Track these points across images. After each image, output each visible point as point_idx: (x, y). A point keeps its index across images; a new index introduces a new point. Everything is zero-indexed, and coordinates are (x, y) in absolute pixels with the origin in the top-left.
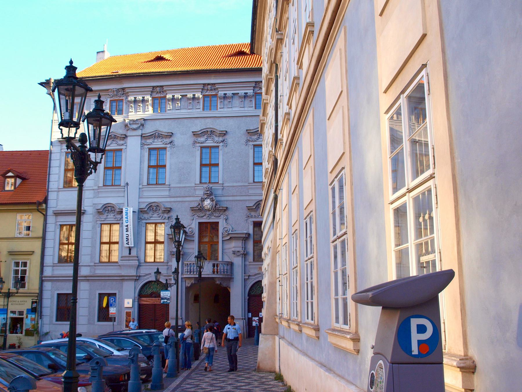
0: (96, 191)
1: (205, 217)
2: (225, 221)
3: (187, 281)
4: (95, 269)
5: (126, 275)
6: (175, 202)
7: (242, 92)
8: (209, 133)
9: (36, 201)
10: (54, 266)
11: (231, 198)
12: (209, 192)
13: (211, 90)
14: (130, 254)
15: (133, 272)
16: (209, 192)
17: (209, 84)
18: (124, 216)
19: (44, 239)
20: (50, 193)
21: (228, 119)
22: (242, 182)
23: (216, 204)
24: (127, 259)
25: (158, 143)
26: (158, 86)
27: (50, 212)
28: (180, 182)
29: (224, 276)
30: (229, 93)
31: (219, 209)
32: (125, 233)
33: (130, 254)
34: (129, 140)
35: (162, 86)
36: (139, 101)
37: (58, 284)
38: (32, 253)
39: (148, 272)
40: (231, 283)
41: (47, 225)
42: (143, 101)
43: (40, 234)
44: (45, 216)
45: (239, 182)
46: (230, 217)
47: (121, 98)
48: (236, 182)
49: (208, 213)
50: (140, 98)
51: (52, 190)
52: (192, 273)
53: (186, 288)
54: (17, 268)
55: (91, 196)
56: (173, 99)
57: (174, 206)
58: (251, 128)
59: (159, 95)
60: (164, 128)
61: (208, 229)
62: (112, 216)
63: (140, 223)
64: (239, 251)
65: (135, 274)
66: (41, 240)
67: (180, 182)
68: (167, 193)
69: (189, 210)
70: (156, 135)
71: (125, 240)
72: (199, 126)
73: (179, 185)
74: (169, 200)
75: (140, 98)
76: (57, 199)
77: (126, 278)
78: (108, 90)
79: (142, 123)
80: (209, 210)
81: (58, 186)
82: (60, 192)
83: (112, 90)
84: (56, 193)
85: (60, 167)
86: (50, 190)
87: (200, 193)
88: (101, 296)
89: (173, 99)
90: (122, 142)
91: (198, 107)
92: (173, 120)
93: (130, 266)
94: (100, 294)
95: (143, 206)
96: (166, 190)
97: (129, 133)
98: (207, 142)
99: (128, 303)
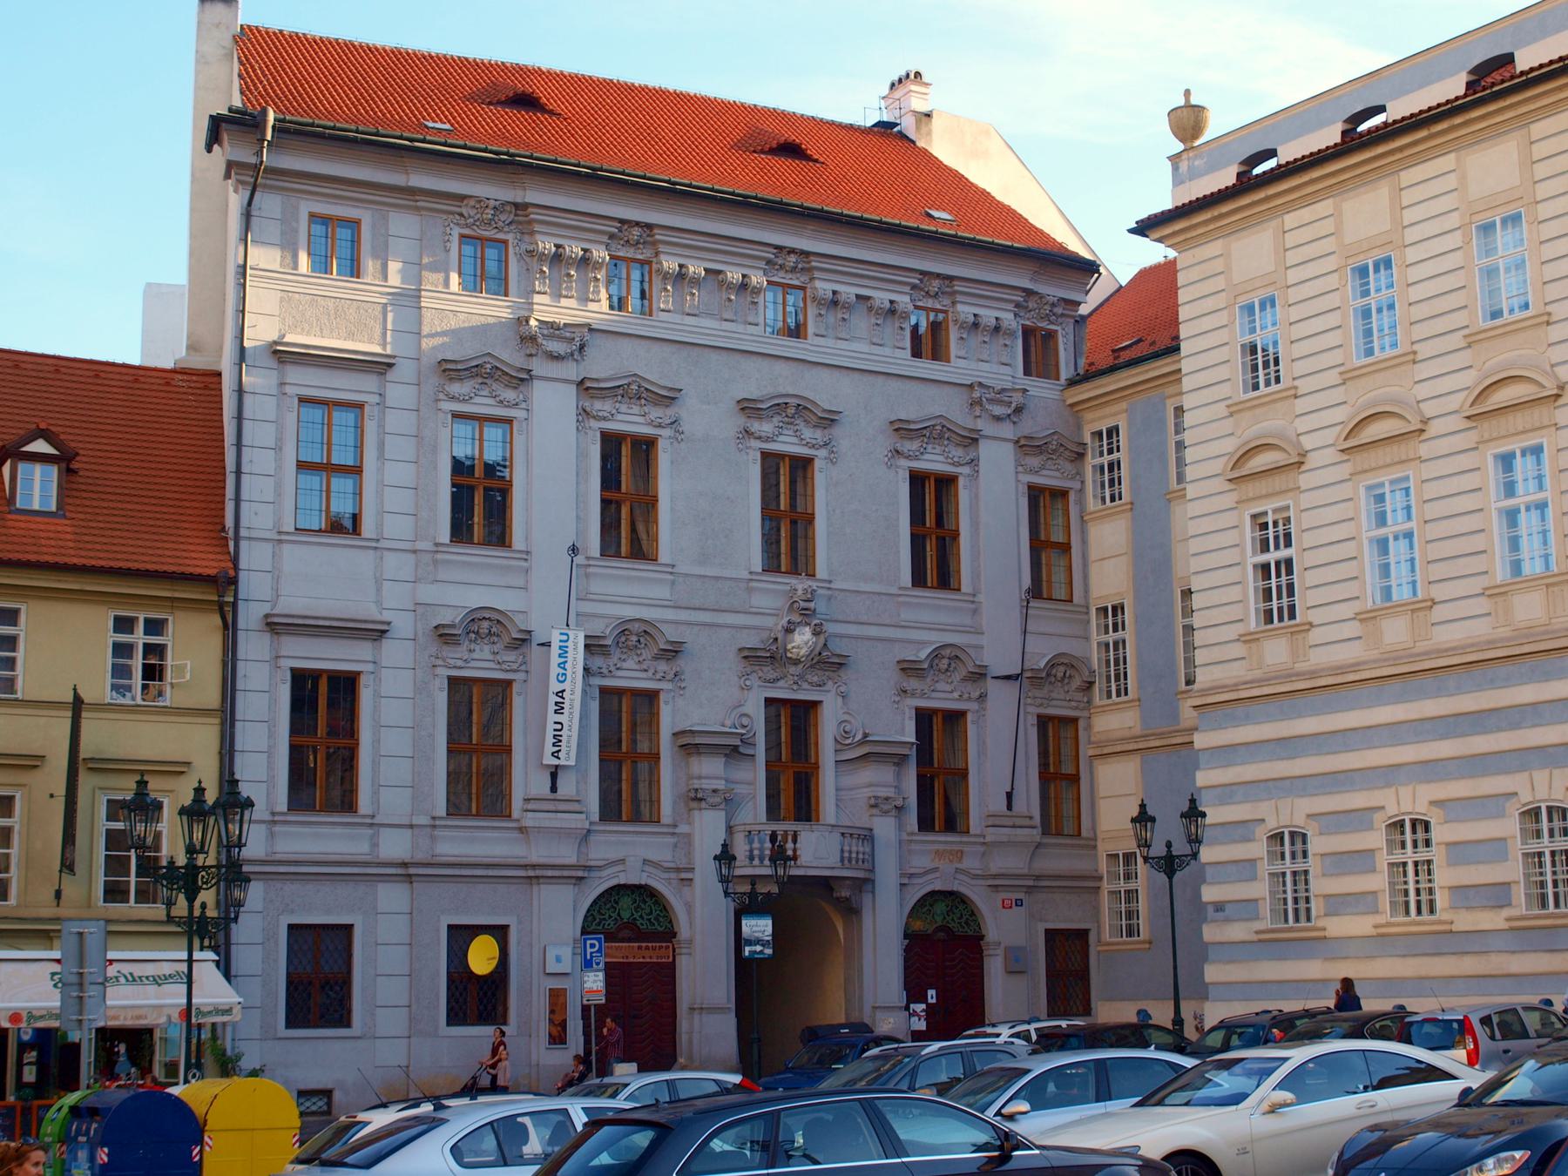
0: (427, 558)
4: (433, 838)
5: (542, 861)
6: (689, 624)
7: (881, 297)
8: (791, 411)
9: (213, 572)
10: (275, 822)
11: (852, 630)
13: (794, 270)
14: (554, 789)
15: (566, 854)
16: (812, 605)
17: (792, 251)
18: (555, 660)
19: (227, 715)
20: (243, 544)
21: (836, 373)
24: (551, 806)
25: (631, 421)
26: (637, 224)
27: (250, 616)
30: (848, 291)
31: (828, 663)
32: (552, 717)
33: (554, 789)
34: (539, 390)
35: (649, 226)
36: (571, 262)
37: (290, 888)
40: (867, 899)
41: (240, 665)
42: (585, 261)
43: (212, 698)
44: (230, 630)
47: (501, 236)
49: (792, 669)
50: (574, 249)
51: (254, 534)
55: (407, 573)
56: (681, 276)
58: (912, 417)
59: (629, 253)
60: (654, 368)
61: (794, 721)
62: (486, 654)
64: (887, 799)
65: (572, 860)
66: (217, 721)
68: (663, 592)
70: (635, 391)
71: (550, 740)
72: (758, 382)
74: (670, 615)
75: (574, 249)
76: (275, 573)
77: (550, 873)
78: (462, 198)
79: (578, 340)
80: (796, 662)
82: (286, 548)
84: (269, 547)
85: (278, 449)
86: (243, 533)
88: (461, 936)
89: (681, 276)
90: (510, 395)
91: (751, 319)
92: (674, 347)
93: (560, 833)
96: (661, 581)
97: (539, 367)
98: (781, 438)
99: (558, 959)
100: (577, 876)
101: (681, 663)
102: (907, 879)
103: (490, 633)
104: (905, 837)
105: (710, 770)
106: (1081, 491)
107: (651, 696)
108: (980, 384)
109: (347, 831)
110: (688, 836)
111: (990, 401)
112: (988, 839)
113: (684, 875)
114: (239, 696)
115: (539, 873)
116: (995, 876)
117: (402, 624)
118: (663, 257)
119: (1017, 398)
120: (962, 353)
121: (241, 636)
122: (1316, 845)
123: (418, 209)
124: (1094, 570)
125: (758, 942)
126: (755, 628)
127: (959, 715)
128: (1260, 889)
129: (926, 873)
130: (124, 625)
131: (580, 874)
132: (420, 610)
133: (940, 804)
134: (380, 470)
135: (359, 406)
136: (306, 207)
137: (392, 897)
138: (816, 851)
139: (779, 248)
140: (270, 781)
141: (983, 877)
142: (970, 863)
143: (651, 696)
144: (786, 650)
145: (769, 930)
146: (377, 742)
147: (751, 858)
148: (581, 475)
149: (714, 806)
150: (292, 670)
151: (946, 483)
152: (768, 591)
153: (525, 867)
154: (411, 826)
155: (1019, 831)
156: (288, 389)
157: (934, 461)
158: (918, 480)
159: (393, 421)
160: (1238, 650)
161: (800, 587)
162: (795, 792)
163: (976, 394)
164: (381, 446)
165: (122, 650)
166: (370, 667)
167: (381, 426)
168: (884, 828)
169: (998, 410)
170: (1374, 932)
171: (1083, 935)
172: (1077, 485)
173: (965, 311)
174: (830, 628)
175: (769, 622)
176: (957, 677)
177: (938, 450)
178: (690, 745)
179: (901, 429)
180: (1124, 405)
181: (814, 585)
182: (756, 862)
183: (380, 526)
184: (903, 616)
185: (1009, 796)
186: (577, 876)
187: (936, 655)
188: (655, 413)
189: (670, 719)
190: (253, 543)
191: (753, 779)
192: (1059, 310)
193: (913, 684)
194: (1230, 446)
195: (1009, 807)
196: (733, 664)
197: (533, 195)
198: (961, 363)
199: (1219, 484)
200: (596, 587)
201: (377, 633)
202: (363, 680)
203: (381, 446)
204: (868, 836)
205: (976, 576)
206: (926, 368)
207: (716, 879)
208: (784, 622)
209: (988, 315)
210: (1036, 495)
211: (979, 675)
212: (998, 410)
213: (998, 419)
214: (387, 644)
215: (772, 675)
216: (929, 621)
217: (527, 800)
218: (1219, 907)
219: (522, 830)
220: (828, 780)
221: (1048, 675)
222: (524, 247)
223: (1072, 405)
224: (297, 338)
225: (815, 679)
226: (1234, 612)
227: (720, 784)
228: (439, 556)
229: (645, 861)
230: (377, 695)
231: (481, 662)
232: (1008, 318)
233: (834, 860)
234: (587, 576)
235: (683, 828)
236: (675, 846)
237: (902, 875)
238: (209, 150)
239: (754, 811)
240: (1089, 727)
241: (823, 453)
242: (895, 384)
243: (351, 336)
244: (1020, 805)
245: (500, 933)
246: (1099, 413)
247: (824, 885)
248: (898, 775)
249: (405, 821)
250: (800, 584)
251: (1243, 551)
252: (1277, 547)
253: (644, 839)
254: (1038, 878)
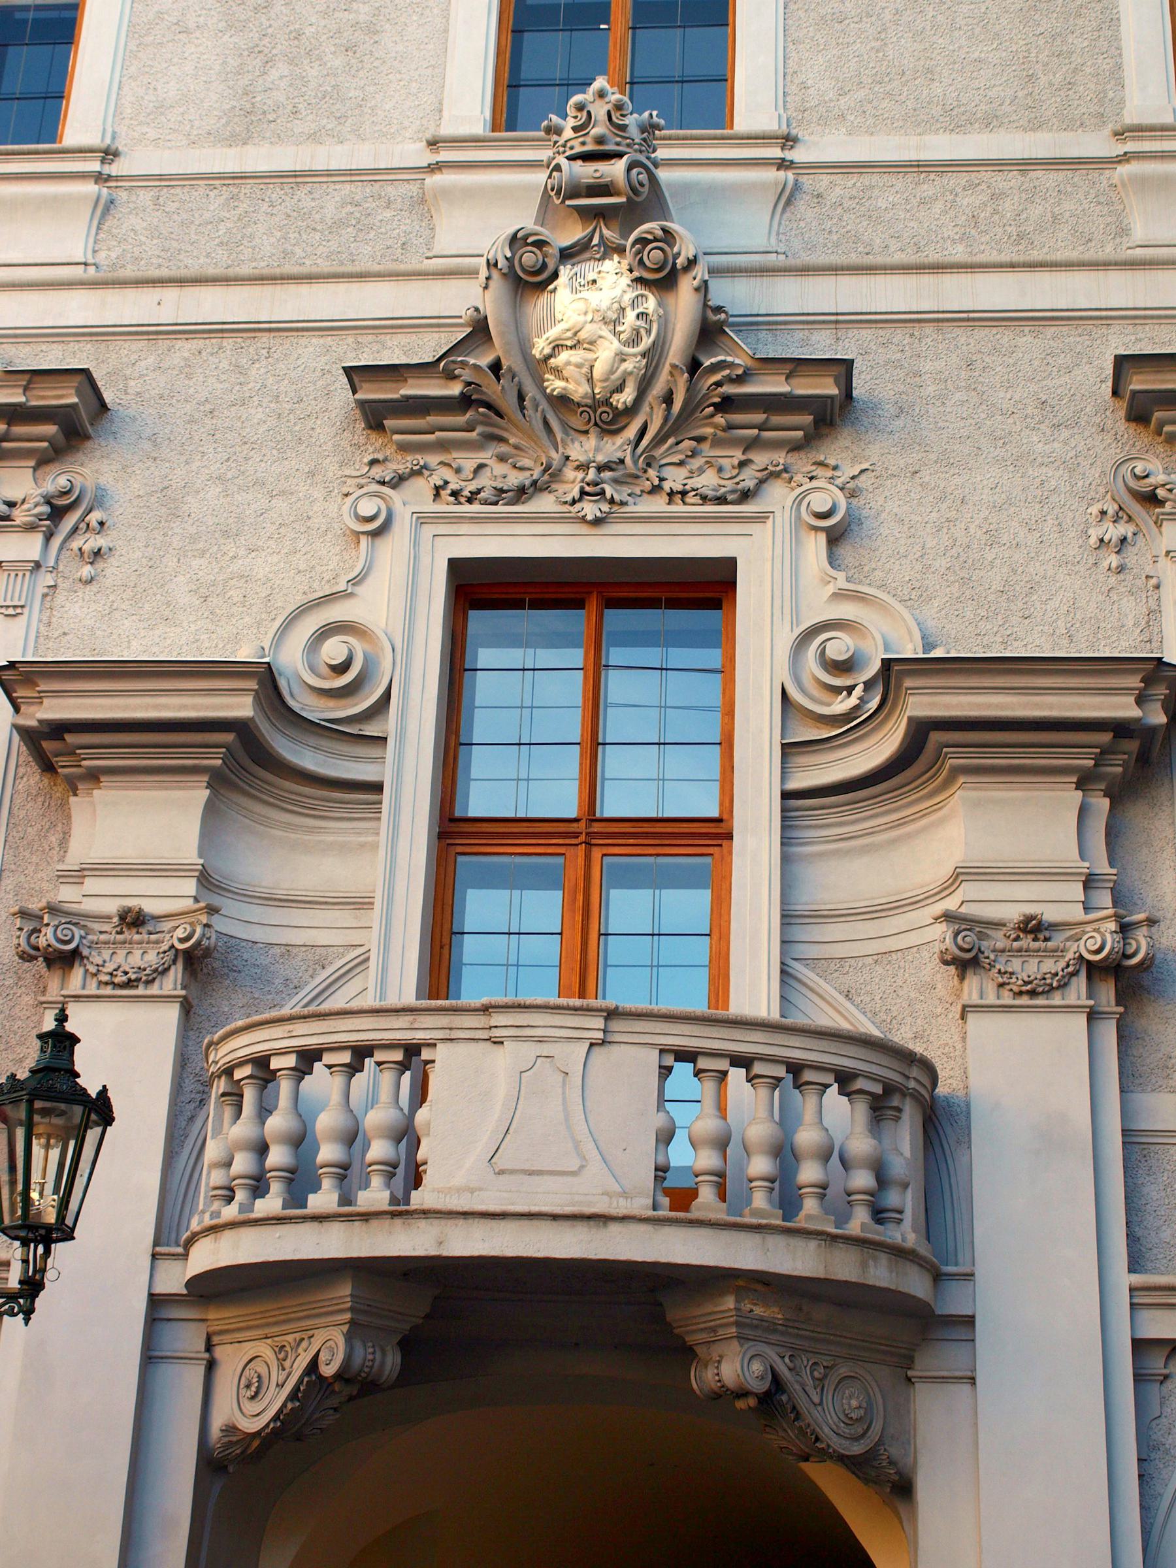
1: (544, 503)
2: (816, 545)
3: (231, 1359)
12: (616, 170)
22: (1036, 125)
23: (710, 331)
28: (248, 122)
29: (844, 1267)
45: (990, 122)
46: (890, 509)
48: (957, 128)
52: (324, 1199)
53: (211, 1465)
57: (124, 378)
64: (1033, 927)
74: (78, 309)
80: (605, 417)
87: (488, 214)
101: (88, 471)
144: (540, 367)
149: (127, 985)
184: (1139, 232)
225: (708, 481)
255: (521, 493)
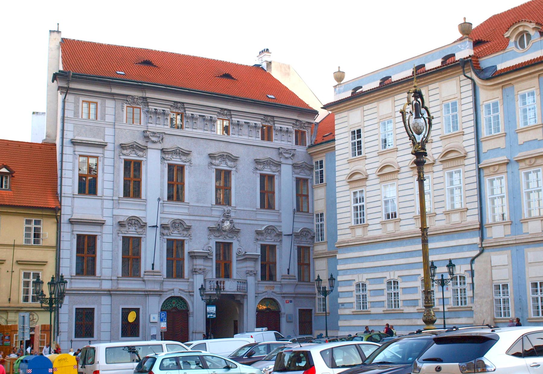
1: (220, 237)
4: (118, 283)
5: (150, 289)
10: (72, 279)
13: (226, 115)
15: (157, 288)
16: (229, 215)
17: (226, 109)
19: (58, 248)
20: (63, 198)
24: (152, 274)
25: (176, 160)
26: (179, 102)
27: (64, 219)
30: (242, 121)
31: (234, 231)
35: (183, 103)
36: (160, 114)
37: (76, 298)
38: (43, 264)
39: (171, 288)
40: (245, 300)
41: (62, 233)
43: (54, 243)
44: (59, 224)
47: (139, 106)
49: (224, 233)
51: (66, 195)
54: (27, 280)
55: (110, 206)
60: (184, 145)
61: (224, 249)
62: (133, 230)
63: (161, 238)
65: (158, 289)
66: (55, 250)
67: (198, 201)
68: (186, 211)
69: (206, 229)
72: (214, 149)
73: (197, 205)
74: (188, 217)
77: (151, 293)
78: (127, 96)
79: (161, 136)
80: (225, 231)
81: (73, 192)
82: (75, 199)
83: (133, 97)
84: (70, 199)
85: (73, 170)
86: (63, 195)
88: (126, 312)
90: (141, 153)
91: (213, 130)
94: (139, 309)
95: (165, 222)
99: (154, 318)
100: (159, 294)
101: (191, 232)
102: (257, 295)
103: (135, 224)
104: (257, 282)
105: (199, 263)
106: (312, 179)
107: (182, 242)
108: (282, 148)
109: (92, 281)
110: (193, 282)
111: (285, 153)
112: (282, 283)
113: (191, 294)
114: (61, 242)
115: (148, 293)
116: (284, 294)
117: (109, 221)
118: (187, 112)
119: (293, 152)
120: (276, 139)
121: (62, 225)
122: (369, 287)
123: (114, 99)
124: (315, 203)
125: (211, 313)
126: (213, 221)
127: (274, 246)
128: (353, 300)
129: (264, 293)
130: (28, 222)
131: (160, 293)
132: (114, 217)
133: (268, 272)
134: (103, 176)
135: (97, 157)
136: (81, 99)
137: (106, 300)
138: (230, 287)
139: (222, 109)
140: (71, 267)
141: (281, 294)
142: (277, 290)
143: (182, 242)
145: (215, 310)
146: (101, 255)
147: (211, 289)
148: (162, 177)
149: (200, 274)
150: (77, 235)
151: (271, 178)
152: (217, 210)
153: (144, 291)
154: (111, 280)
155: (291, 280)
156: (76, 153)
157: (267, 171)
158: (262, 176)
159: (107, 162)
160: (349, 231)
161: (226, 209)
162: (224, 270)
163: (280, 151)
164: (103, 169)
165: (28, 229)
166: (100, 234)
167: (103, 163)
168: (251, 280)
169: (287, 156)
170: (383, 312)
171: (311, 310)
172: (311, 178)
173: (278, 126)
174: (235, 221)
175: (217, 219)
176: (273, 235)
177: (269, 167)
178: (193, 256)
179: (257, 162)
180: (324, 154)
181: (230, 208)
182: (212, 290)
183: (103, 192)
185: (288, 270)
186: (159, 294)
187: (267, 228)
188: (184, 158)
189: (187, 248)
190: (66, 198)
191: (213, 264)
192: (306, 125)
193: (259, 237)
194: (348, 172)
195: (288, 273)
196: (206, 232)
197: (149, 95)
198: (276, 142)
199: (345, 183)
200: (166, 210)
201: (101, 224)
202: (98, 237)
203: (103, 169)
204: (245, 282)
205: (280, 205)
206: (266, 143)
207: (199, 295)
208: (221, 220)
209: (285, 127)
210: (298, 180)
211: (280, 235)
212: (287, 156)
213: (287, 158)
214: (104, 227)
215: (218, 235)
216: (266, 219)
217: (145, 272)
218: (343, 304)
219: (144, 281)
220: (235, 265)
221: (301, 234)
222: (145, 109)
223: (309, 154)
224: (79, 138)
226: (348, 220)
227: (202, 267)
228: (120, 201)
229: (180, 290)
230: (102, 242)
231: (132, 232)
232: (290, 127)
233: (235, 289)
234: (163, 206)
235: (191, 280)
236: (189, 285)
237: (256, 293)
238: (53, 81)
239: (212, 275)
240: (313, 250)
241: (234, 169)
242: (256, 148)
243: (94, 137)
244: (291, 273)
245: (137, 310)
246: (317, 156)
247: (232, 297)
248: (255, 264)
249: (110, 278)
250: (226, 208)
251: (351, 203)
252: (360, 202)
253: (179, 283)
254: (297, 294)
255: (219, 236)
